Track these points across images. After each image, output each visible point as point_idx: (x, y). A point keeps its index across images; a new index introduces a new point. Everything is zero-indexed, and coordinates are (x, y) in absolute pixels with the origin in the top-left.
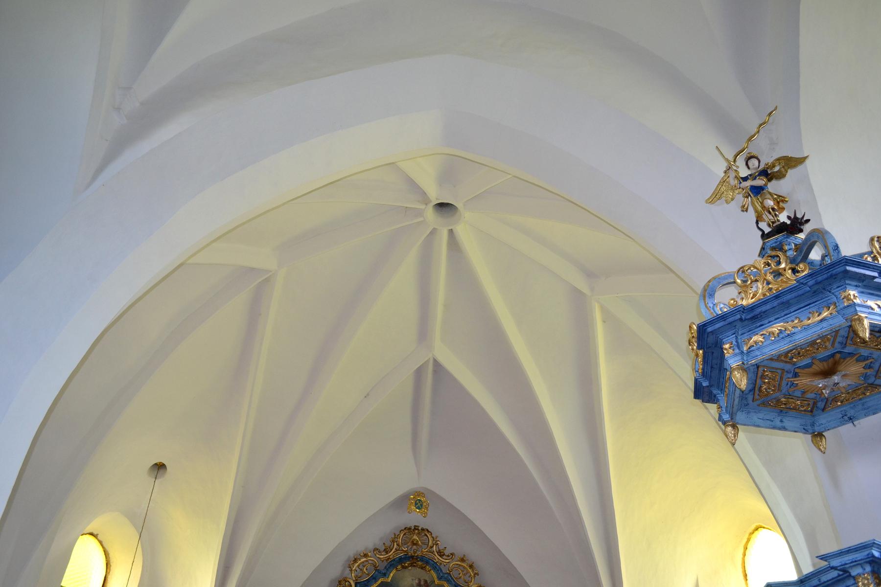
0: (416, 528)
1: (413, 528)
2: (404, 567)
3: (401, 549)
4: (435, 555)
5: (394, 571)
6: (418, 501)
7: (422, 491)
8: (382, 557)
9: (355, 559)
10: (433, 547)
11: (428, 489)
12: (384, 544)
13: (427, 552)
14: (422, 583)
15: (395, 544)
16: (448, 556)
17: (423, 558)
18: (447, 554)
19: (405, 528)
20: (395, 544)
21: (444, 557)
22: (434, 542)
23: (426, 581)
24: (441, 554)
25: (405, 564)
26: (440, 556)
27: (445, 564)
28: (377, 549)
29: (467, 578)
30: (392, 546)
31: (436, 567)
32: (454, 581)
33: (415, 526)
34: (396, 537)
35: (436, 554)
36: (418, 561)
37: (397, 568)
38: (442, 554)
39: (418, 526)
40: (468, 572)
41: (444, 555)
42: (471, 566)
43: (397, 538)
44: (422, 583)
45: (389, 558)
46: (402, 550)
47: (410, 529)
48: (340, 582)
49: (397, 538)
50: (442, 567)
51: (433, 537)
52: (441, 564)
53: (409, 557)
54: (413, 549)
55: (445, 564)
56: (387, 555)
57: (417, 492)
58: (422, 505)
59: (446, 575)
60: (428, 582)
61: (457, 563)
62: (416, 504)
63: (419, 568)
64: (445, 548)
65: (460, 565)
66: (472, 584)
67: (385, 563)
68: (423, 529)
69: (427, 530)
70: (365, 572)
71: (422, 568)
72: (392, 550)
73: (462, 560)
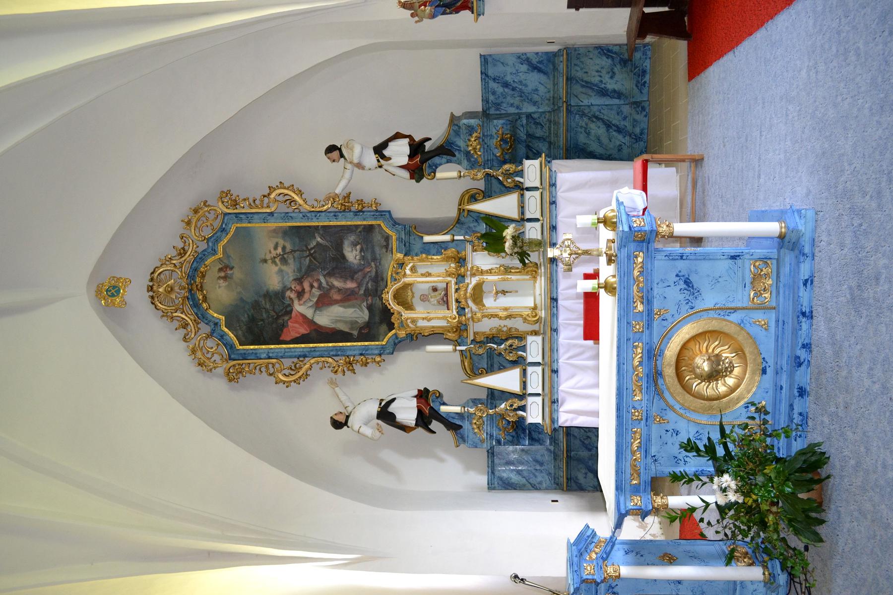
0: (150, 288)
1: (151, 293)
2: (205, 299)
3: (181, 307)
4: (185, 260)
5: (211, 312)
6: (109, 293)
7: (94, 288)
8: (193, 330)
9: (199, 365)
10: (174, 264)
11: (89, 283)
12: (176, 329)
13: (181, 272)
14: (222, 274)
15: (175, 314)
16: (185, 242)
17: (191, 277)
18: (182, 245)
19: (152, 303)
20: (175, 314)
21: (186, 248)
22: (167, 263)
23: (220, 270)
24: (182, 252)
25: (199, 300)
26: (185, 254)
27: (195, 246)
28: (185, 337)
29: (211, 216)
30: (179, 319)
31: (200, 258)
32: (216, 233)
33: (148, 291)
34: (165, 315)
35: (183, 259)
36: (195, 282)
37: (207, 309)
38: (182, 251)
39: (148, 286)
40: (204, 216)
41: (183, 249)
42: (196, 211)
43: (167, 313)
44: (222, 274)
45: (195, 321)
46: (183, 304)
47: (152, 297)
48: (230, 381)
49: (167, 313)
50: (200, 250)
51: (162, 265)
52: (196, 252)
53: (191, 295)
54: (179, 290)
55: (195, 246)
56: (191, 323)
57: (96, 296)
58: (114, 287)
59: (210, 244)
60: (221, 266)
61: (193, 231)
62: (113, 295)
63: (204, 280)
64: (174, 247)
65: (196, 226)
66: (218, 210)
67: (202, 325)
68: (152, 280)
69: (152, 273)
70: (216, 350)
71: (203, 276)
72: (183, 318)
73: (189, 223)
